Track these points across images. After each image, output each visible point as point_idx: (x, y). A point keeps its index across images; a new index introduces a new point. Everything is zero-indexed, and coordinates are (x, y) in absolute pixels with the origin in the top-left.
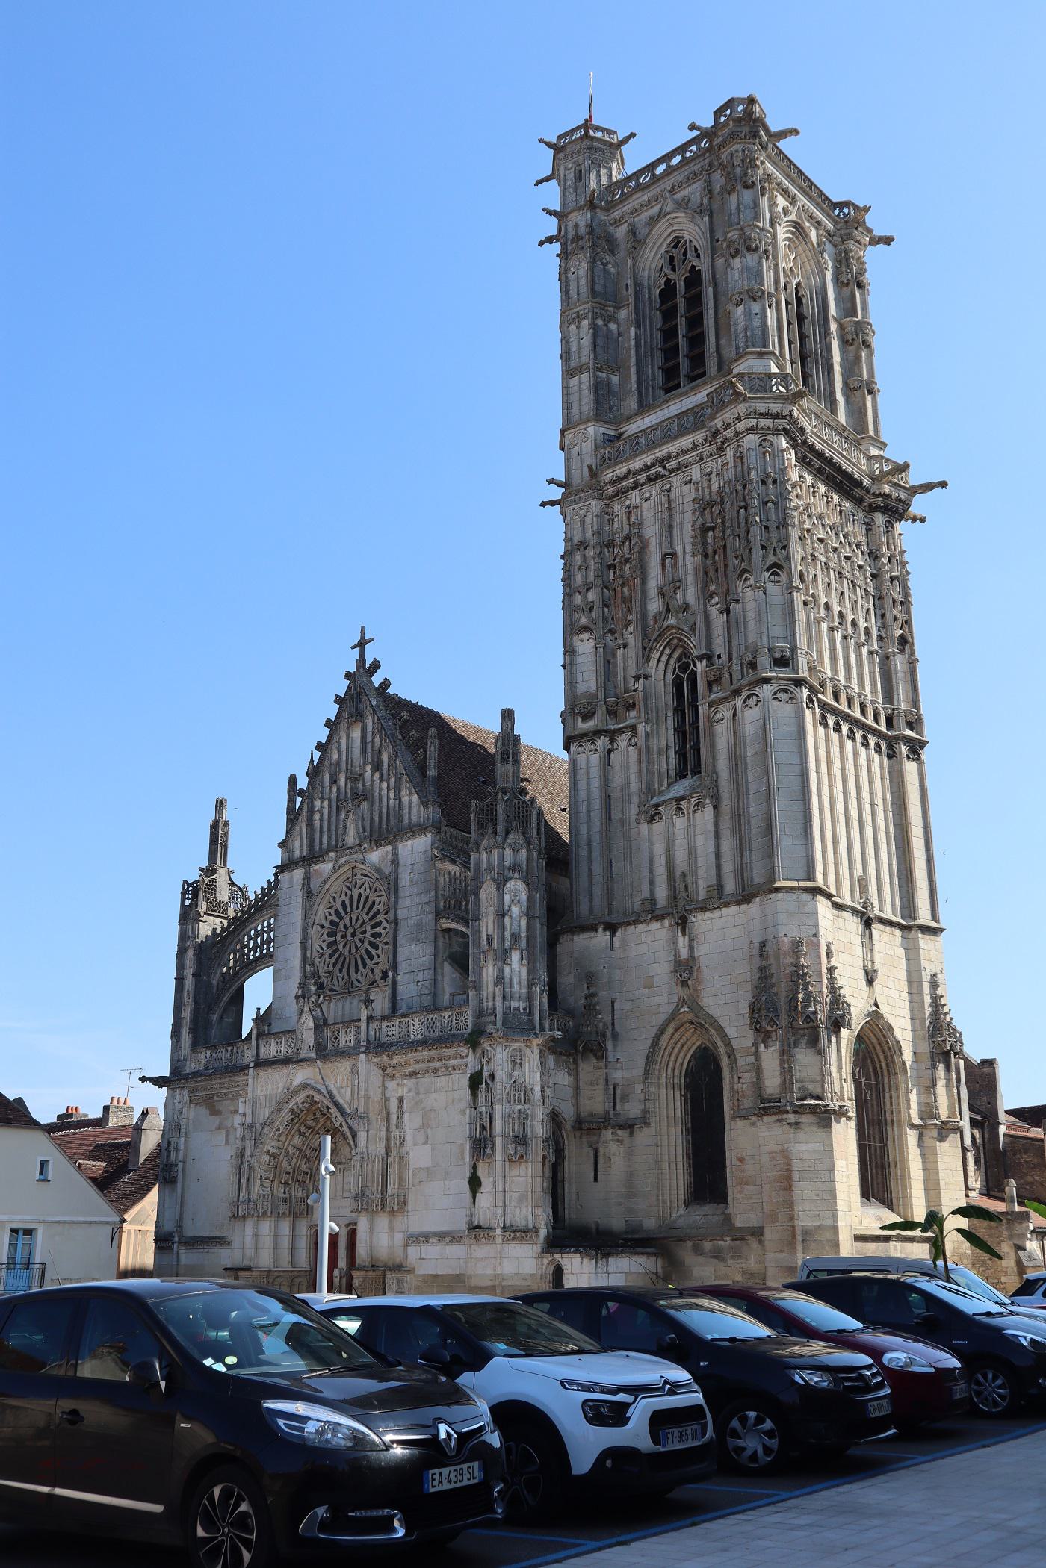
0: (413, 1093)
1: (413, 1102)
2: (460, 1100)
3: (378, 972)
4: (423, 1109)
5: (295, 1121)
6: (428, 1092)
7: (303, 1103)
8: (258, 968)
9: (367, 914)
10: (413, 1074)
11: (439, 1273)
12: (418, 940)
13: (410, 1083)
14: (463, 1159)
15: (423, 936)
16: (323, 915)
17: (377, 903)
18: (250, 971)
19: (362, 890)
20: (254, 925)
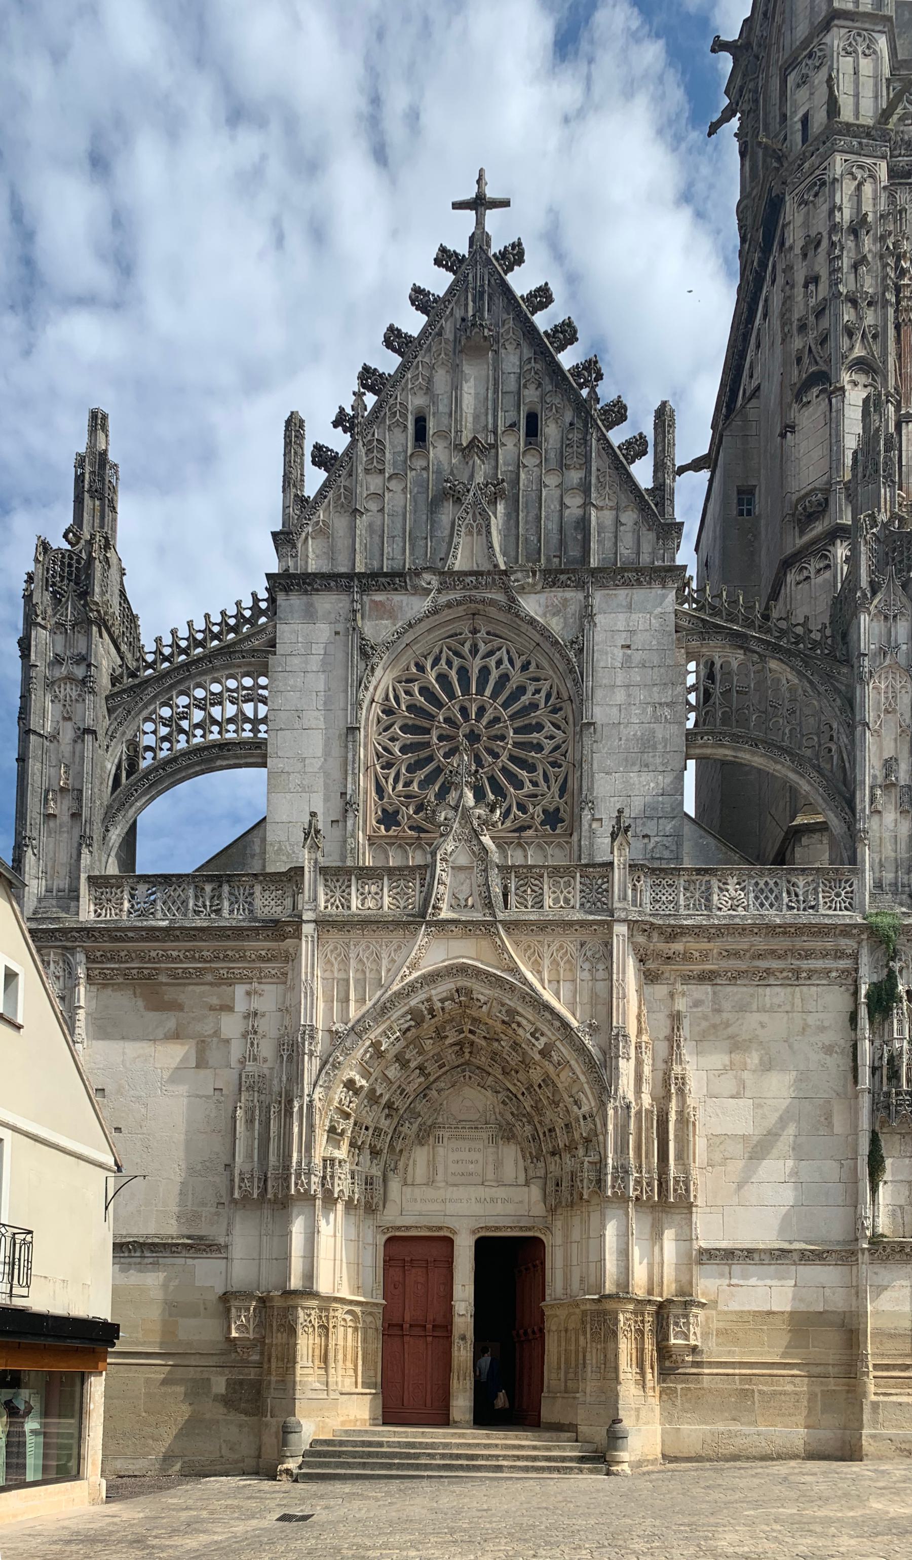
0: (706, 1008)
1: (704, 1024)
2: (822, 1029)
3: (537, 812)
4: (729, 1037)
5: (409, 1034)
6: (742, 1008)
7: (442, 1001)
8: (219, 763)
9: (505, 705)
10: (706, 977)
11: (775, 1309)
12: (647, 766)
13: (703, 991)
14: (830, 1125)
15: (658, 760)
16: (391, 689)
17: (531, 689)
18: (203, 762)
19: (492, 662)
20: (208, 678)
